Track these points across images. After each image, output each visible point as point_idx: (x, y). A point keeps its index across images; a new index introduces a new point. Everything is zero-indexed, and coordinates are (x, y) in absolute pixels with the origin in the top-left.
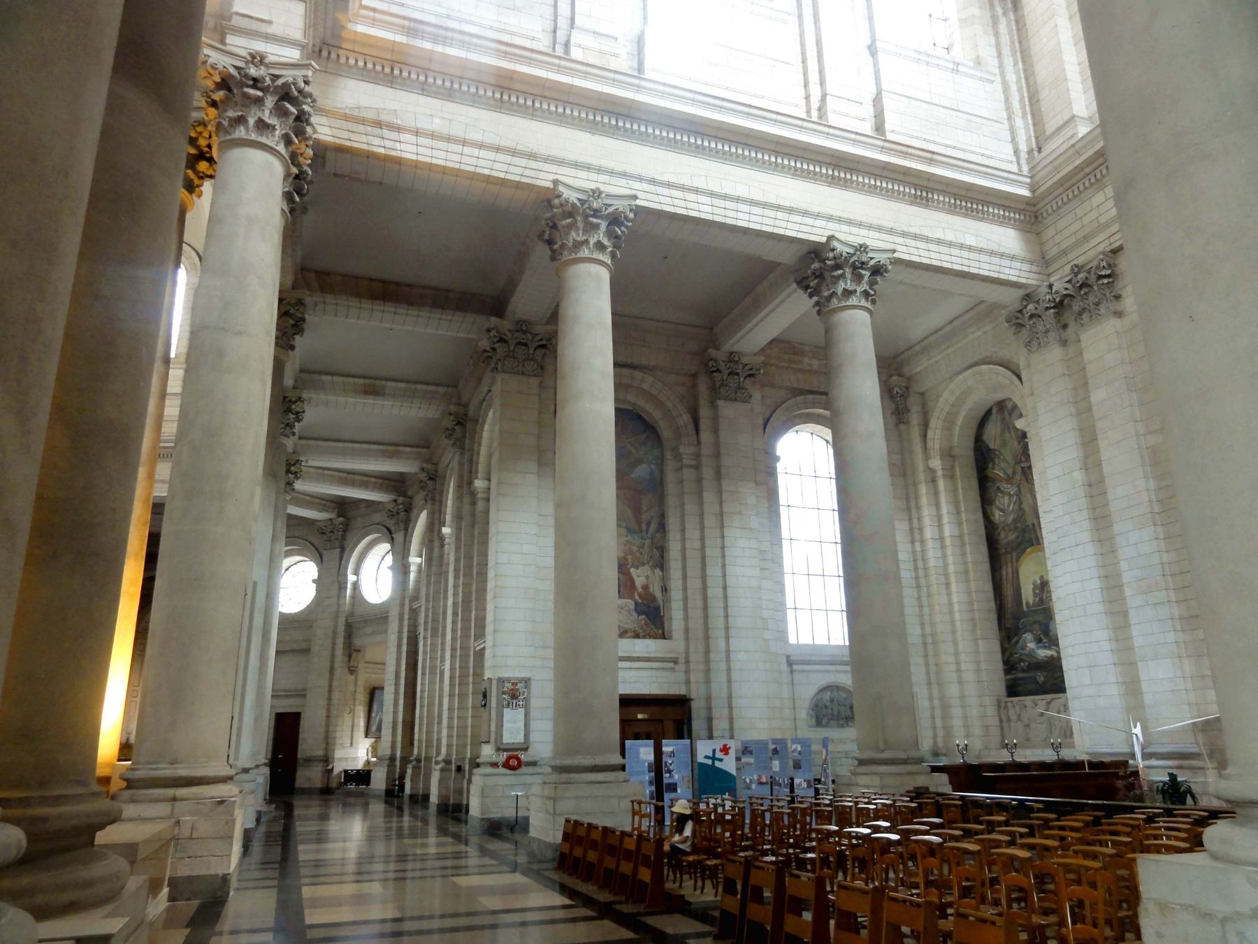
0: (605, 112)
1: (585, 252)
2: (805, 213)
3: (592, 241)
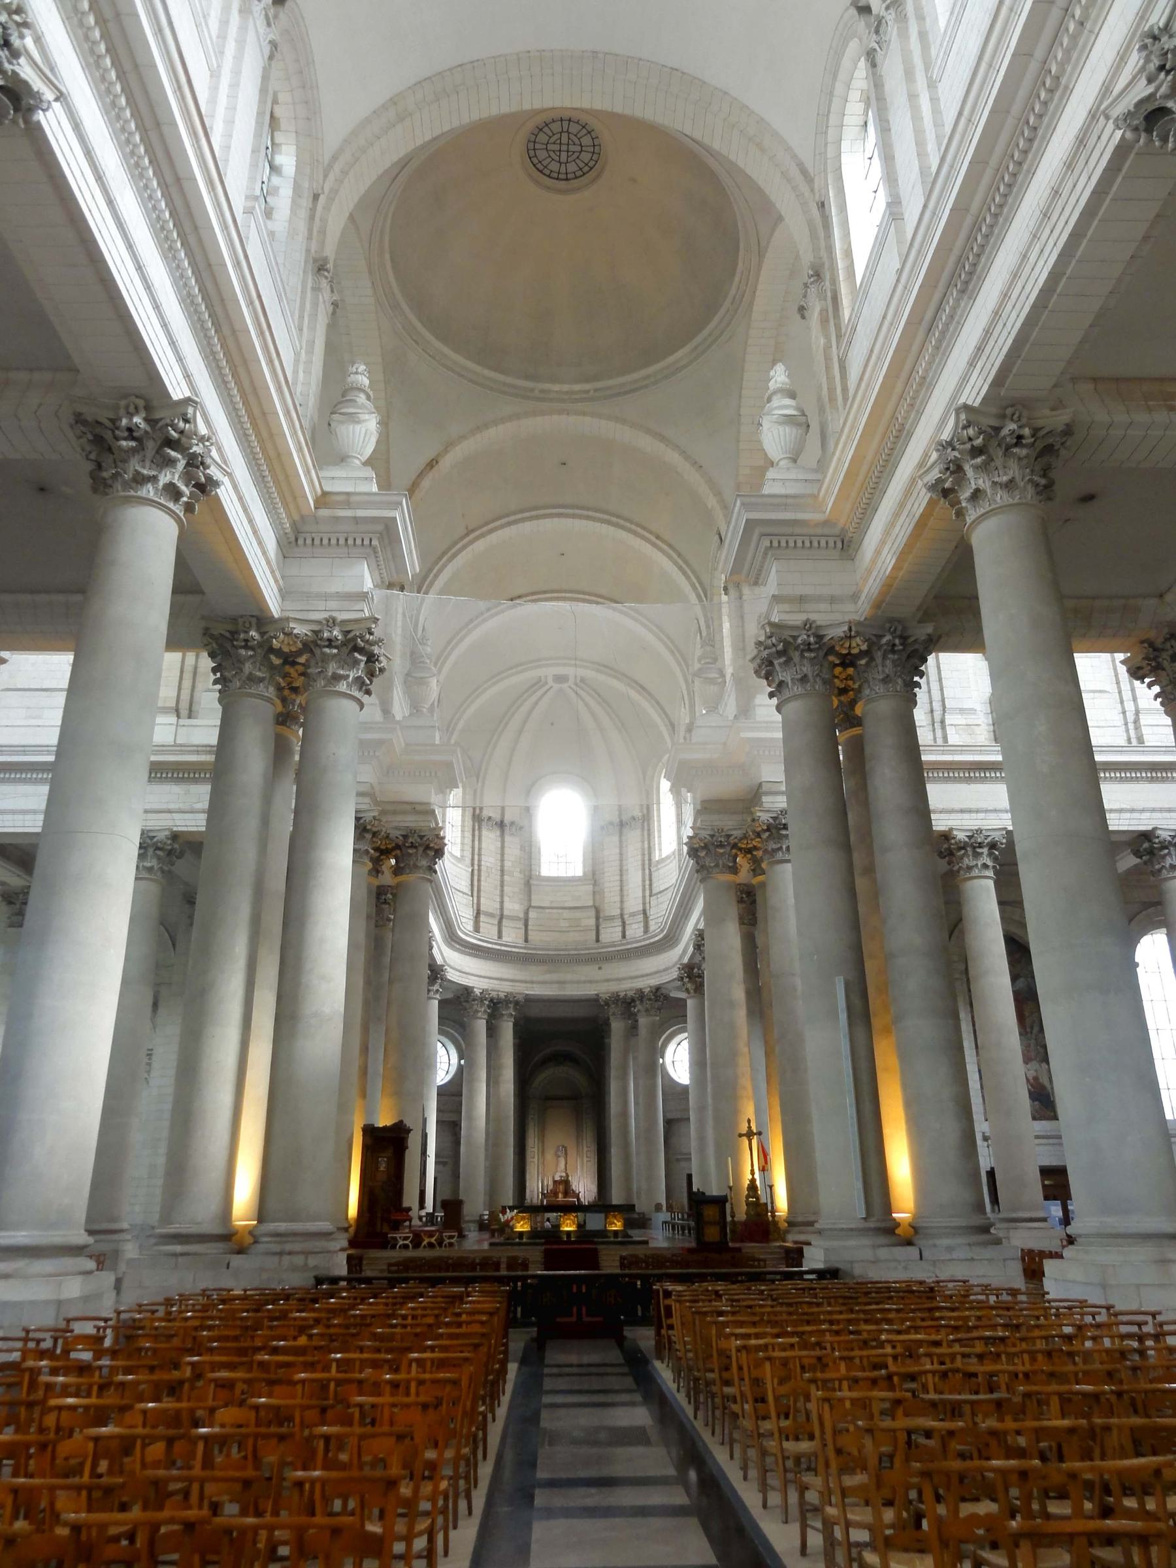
0: (974, 770)
1: (975, 872)
2: (1132, 811)
3: (979, 864)
